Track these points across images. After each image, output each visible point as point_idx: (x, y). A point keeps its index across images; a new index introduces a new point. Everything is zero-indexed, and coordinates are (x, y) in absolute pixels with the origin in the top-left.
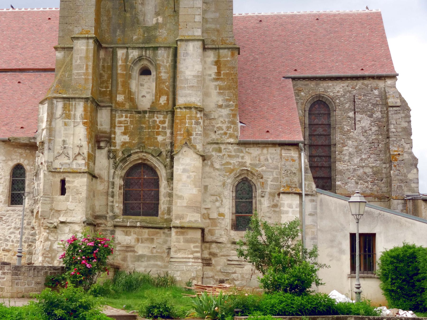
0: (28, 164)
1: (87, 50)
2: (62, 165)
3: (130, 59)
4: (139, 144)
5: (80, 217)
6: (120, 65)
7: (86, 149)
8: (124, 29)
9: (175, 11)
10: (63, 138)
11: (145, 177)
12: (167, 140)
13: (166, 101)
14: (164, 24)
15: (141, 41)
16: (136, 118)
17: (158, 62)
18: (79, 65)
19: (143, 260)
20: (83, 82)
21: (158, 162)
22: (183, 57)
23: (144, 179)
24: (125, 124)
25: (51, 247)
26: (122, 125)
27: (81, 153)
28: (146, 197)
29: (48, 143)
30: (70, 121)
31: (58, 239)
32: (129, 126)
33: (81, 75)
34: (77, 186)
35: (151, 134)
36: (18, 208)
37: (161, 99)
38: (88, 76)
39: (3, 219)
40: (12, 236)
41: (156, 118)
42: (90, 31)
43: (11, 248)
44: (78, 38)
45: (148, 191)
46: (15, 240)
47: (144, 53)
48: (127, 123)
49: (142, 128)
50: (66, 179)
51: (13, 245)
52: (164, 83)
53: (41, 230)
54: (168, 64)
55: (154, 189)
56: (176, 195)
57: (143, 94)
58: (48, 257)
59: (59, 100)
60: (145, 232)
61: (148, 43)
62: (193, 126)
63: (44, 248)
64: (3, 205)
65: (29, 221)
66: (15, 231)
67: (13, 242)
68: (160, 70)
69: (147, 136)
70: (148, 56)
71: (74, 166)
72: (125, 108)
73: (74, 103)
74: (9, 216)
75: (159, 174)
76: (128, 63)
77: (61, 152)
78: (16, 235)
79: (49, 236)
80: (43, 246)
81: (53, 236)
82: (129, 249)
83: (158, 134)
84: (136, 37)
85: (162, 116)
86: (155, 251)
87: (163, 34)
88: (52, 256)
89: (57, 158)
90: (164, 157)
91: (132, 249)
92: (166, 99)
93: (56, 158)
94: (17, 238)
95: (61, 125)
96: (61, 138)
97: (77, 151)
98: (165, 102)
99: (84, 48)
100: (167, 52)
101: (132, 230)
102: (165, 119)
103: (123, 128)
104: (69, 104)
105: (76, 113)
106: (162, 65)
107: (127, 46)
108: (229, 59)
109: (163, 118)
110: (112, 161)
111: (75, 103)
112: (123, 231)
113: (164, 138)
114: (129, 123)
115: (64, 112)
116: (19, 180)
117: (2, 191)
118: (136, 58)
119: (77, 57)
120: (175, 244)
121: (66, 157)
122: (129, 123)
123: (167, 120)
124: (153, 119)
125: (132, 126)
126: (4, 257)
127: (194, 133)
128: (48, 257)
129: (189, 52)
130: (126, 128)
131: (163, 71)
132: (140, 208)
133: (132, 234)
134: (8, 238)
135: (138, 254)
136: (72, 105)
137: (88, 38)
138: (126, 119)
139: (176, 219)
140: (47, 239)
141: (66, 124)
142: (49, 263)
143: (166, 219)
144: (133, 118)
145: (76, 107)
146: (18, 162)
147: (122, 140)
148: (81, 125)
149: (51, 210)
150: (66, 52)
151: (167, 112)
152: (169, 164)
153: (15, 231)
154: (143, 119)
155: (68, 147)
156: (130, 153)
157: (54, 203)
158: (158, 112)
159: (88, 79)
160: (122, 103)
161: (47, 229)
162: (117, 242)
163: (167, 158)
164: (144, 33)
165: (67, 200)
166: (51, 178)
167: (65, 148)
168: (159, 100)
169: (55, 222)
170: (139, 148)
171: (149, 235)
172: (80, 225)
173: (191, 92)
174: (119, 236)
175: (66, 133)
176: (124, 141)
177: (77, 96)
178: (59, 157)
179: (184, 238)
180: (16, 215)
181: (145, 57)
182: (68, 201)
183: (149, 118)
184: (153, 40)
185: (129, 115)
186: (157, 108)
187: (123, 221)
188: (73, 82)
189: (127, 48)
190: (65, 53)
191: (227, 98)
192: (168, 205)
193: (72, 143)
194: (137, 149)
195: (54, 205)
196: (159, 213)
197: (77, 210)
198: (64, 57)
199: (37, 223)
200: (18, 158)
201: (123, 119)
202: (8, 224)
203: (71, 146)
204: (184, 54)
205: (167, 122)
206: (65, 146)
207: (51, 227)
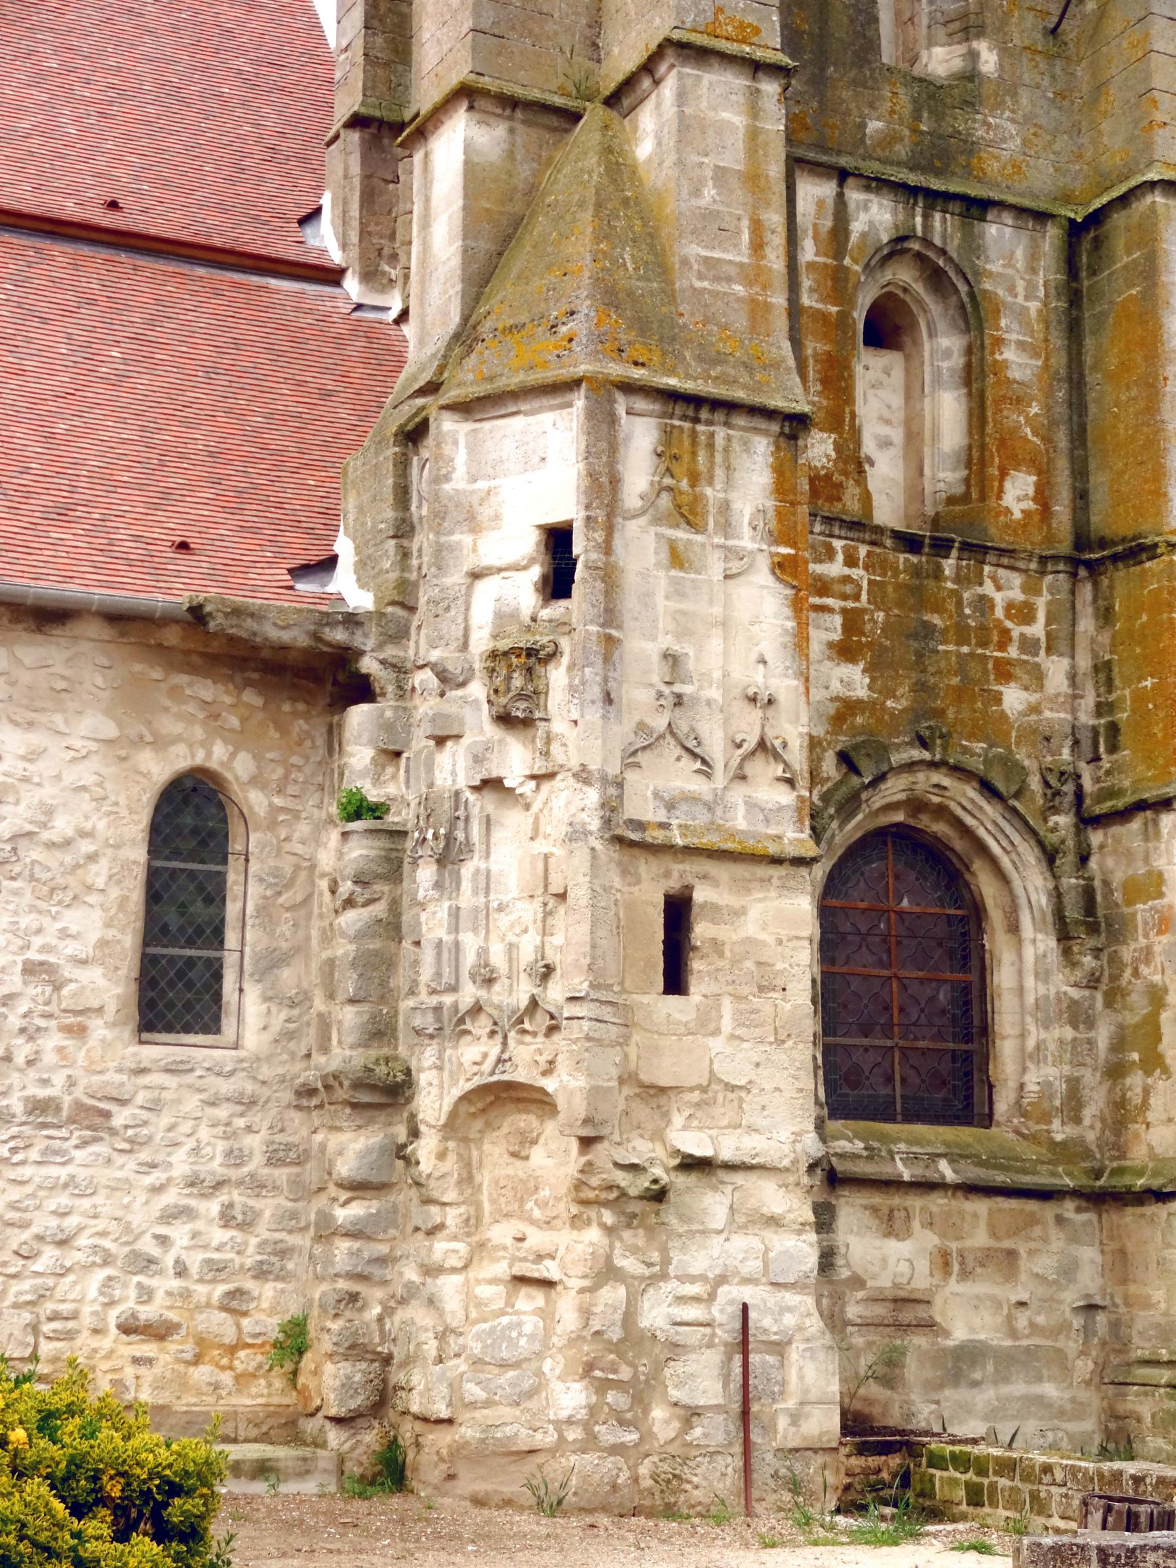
0: (256, 781)
1: (753, 134)
2: (671, 806)
3: (854, 238)
4: (917, 719)
5: (785, 1135)
6: (811, 265)
7: (796, 720)
8: (823, 70)
9: (1054, 31)
10: (666, 642)
11: (905, 903)
12: (1048, 714)
13: (1034, 499)
14: (1008, 87)
15: (901, 151)
16: (896, 572)
17: (987, 285)
18: (710, 215)
19: (977, 1376)
20: (740, 321)
23: (901, 914)
24: (844, 597)
25: (629, 1317)
26: (830, 601)
28: (914, 1019)
29: (599, 661)
30: (699, 538)
31: (672, 1270)
32: (864, 611)
33: (729, 279)
34: (763, 944)
35: (974, 669)
37: (1008, 485)
38: (764, 288)
39: (118, 1121)
40: (180, 1233)
41: (988, 588)
42: (757, 31)
43: (173, 1316)
45: (922, 981)
46: (195, 1261)
47: (919, 220)
48: (857, 597)
49: (928, 630)
51: (186, 1294)
52: (1019, 400)
53: (478, 1206)
54: (1034, 306)
55: (948, 975)
58: (619, 1385)
59: (641, 404)
60: (975, 1216)
61: (938, 173)
63: (596, 1325)
64: (108, 1034)
65: (279, 1138)
66: (193, 1203)
67: (181, 1271)
68: (998, 328)
69: (955, 681)
70: (937, 241)
71: (740, 821)
72: (844, 512)
73: (721, 433)
74: (154, 1107)
75: (987, 887)
76: (847, 261)
77: (660, 723)
78: (199, 1225)
79: (612, 1247)
80: (586, 1314)
81: (634, 1250)
83: (1005, 672)
84: (879, 125)
85: (1017, 579)
86: (1022, 1320)
87: (1004, 140)
88: (635, 1376)
89: (640, 758)
90: (1033, 800)
91: (921, 1312)
92: (1031, 491)
93: (631, 758)
94: (205, 1247)
95: (652, 559)
97: (749, 725)
98: (1030, 505)
99: (737, 119)
100: (1025, 236)
101: (915, 1202)
102: (1033, 599)
103: (838, 620)
104: (694, 434)
105: (732, 496)
106: (1004, 303)
107: (844, 161)
109: (1025, 589)
111: (729, 439)
112: (875, 1210)
113: (1034, 698)
114: (864, 596)
115: (668, 481)
116: (192, 874)
117: (103, 943)
118: (885, 238)
119: (701, 165)
121: (686, 759)
122: (864, 596)
123: (1041, 604)
125: (880, 616)
126: (130, 1371)
128: (619, 1385)
130: (852, 622)
131: (1014, 337)
132: (890, 1079)
133: (916, 1224)
134: (155, 1251)
135: (950, 1343)
136: (711, 446)
137: (756, 67)
138: (847, 571)
140: (607, 1272)
141: (677, 558)
142: (622, 1423)
143: (1064, 1144)
144: (884, 575)
145: (734, 463)
146: (199, 759)
147: (836, 688)
148: (763, 576)
150: (521, 129)
151: (1043, 560)
152: (1070, 843)
153: (193, 1203)
154: (931, 583)
155: (695, 699)
156: (885, 768)
157: (636, 1038)
158: (1002, 552)
159: (768, 307)
160: (828, 477)
161: (606, 1204)
162: (845, 1274)
164: (917, 117)
165: (706, 1024)
166: (617, 882)
167: (679, 700)
168: (1001, 490)
169: (652, 1161)
170: (924, 744)
171: (993, 1233)
172: (791, 1179)
174: (852, 1240)
175: (684, 613)
176: (844, 692)
177: (739, 395)
178: (648, 754)
180: (192, 1102)
181: (916, 246)
182: (716, 1032)
183: (957, 579)
184: (962, 160)
185: (863, 550)
186: (993, 531)
187: (872, 1155)
188: (688, 315)
189: (843, 175)
190: (512, 131)
192: (1066, 1069)
193: (717, 675)
194: (910, 744)
195: (632, 1051)
196: (1002, 1107)
197: (768, 1087)
198: (511, 155)
199: (452, 1158)
200: (198, 733)
201: (835, 568)
202: (144, 1155)
203: (715, 694)
205: (1041, 616)
206: (678, 688)
207: (633, 1192)
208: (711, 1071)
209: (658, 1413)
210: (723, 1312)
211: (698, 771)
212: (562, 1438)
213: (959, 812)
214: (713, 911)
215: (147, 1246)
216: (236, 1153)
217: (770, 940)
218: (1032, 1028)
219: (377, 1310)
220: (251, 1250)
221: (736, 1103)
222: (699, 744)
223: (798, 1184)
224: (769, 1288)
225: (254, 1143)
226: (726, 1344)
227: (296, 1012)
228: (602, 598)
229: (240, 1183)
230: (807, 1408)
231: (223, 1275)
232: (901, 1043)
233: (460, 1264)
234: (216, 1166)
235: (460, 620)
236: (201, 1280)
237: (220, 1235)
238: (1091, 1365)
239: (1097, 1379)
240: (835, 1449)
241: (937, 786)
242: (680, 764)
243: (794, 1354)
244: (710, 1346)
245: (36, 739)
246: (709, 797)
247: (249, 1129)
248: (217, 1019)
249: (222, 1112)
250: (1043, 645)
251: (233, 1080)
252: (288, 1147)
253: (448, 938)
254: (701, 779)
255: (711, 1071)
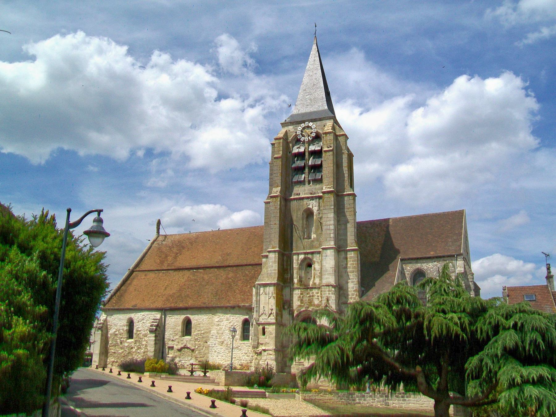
3: (299, 259)
5: (272, 347)
10: (263, 305)
25: (258, 363)
36: (246, 342)
40: (244, 357)
57: (308, 277)
82: (301, 364)
85: (317, 290)
91: (302, 364)
107: (298, 252)
108: (352, 255)
110: (291, 316)
129: (328, 254)
180: (245, 346)
202: (241, 351)
210: (266, 362)
215: (241, 358)
234: (247, 352)
237: (247, 357)
245: (233, 317)
249: (247, 347)
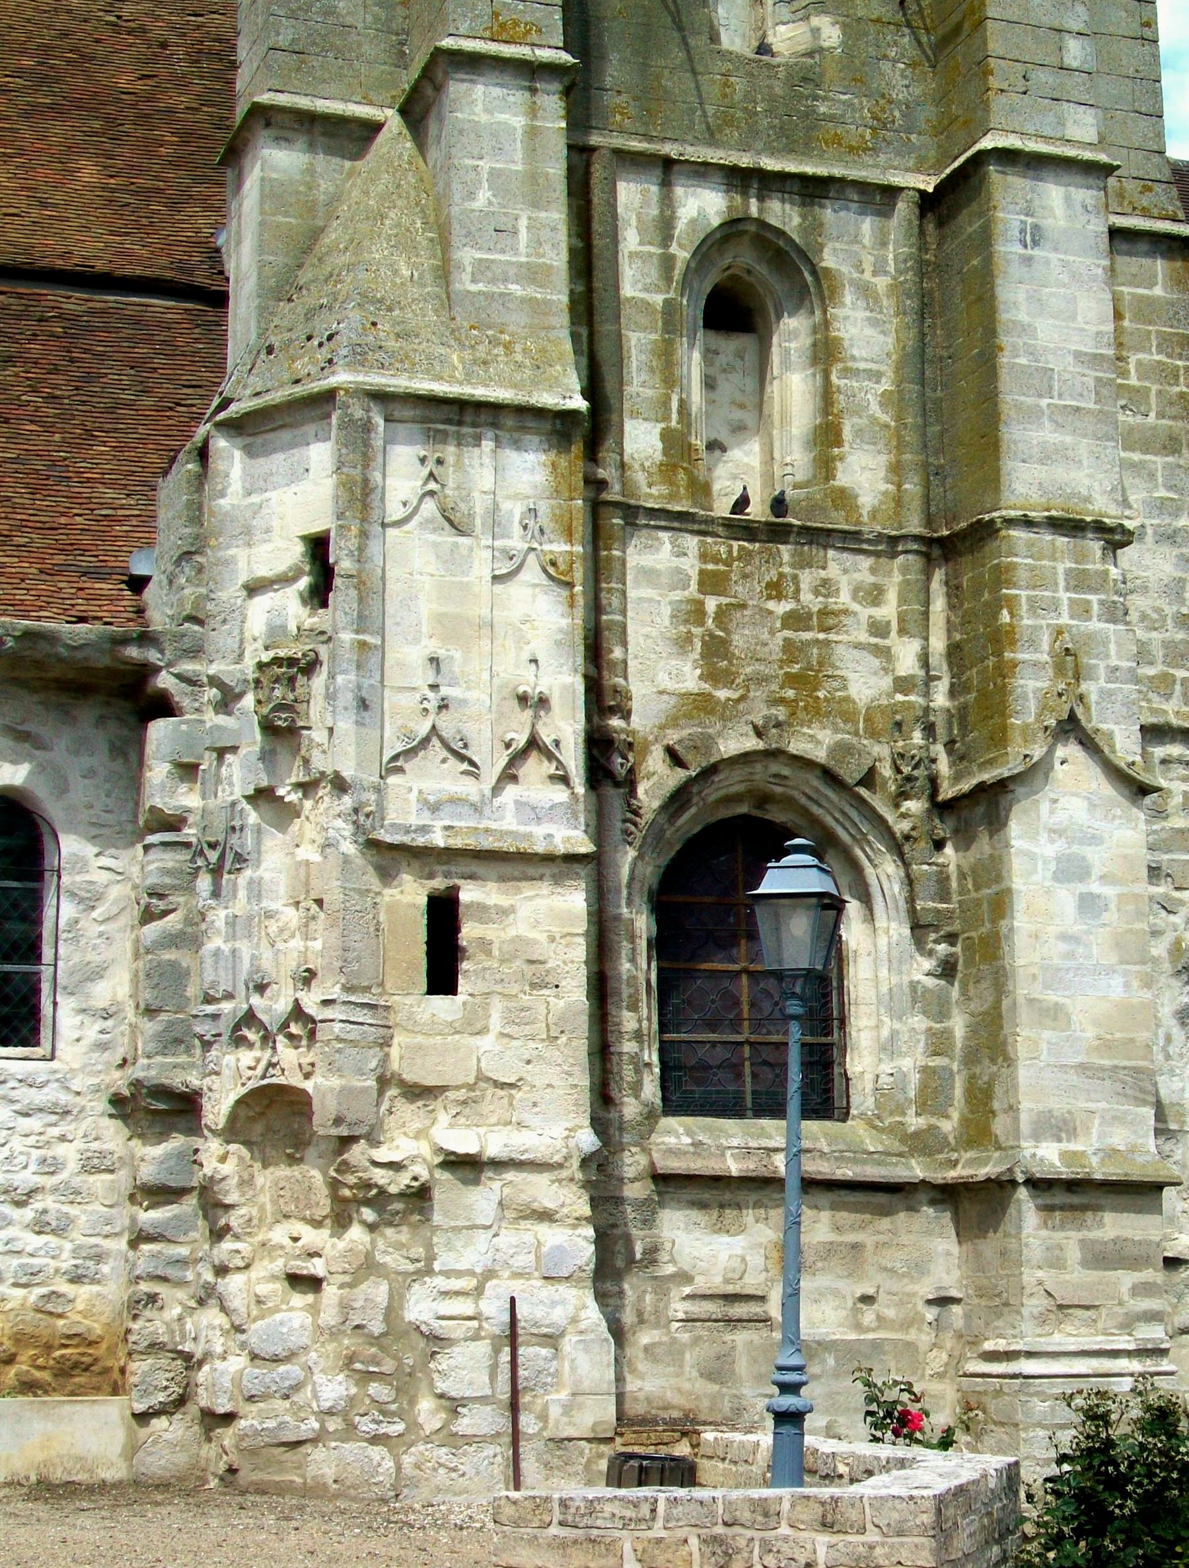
1: (532, 133)
3: (681, 226)
10: (432, 646)
21: (854, 814)
22: (1018, 249)
25: (392, 1312)
27: (548, 741)
28: (766, 1013)
31: (437, 1266)
34: (536, 942)
41: (833, 571)
44: (473, 63)
50: (465, 897)
54: (882, 283)
56: (1031, 1001)
62: (1095, 625)
76: (674, 249)
77: (423, 729)
81: (399, 1246)
82: (740, 1310)
85: (866, 562)
86: (868, 1316)
91: (753, 1309)
96: (417, 641)
107: (670, 149)
108: (1158, 291)
109: (873, 571)
115: (432, 486)
120: (1040, 1274)
121: (452, 761)
124: (823, 573)
127: (1102, 665)
129: (1047, 223)
139: (1037, 1136)
143: (917, 1134)
149: (384, 1082)
155: (463, 702)
162: (670, 1269)
163: (903, 795)
165: (474, 1025)
169: (413, 1159)
173: (1068, 439)
179: (1082, 1242)
191: (1162, 493)
197: (540, 1082)
204: (1023, 231)
205: (892, 596)
208: (479, 1069)
209: (425, 1405)
210: (494, 1309)
211: (464, 773)
212: (323, 1427)
213: (803, 800)
214: (481, 910)
216: (49, 1161)
217: (542, 938)
218: (887, 1020)
219: (177, 1311)
220: (65, 1255)
221: (506, 1100)
222: (466, 746)
223: (572, 1180)
224: (540, 1283)
225: (69, 1153)
226: (494, 1337)
227: (110, 1023)
228: (355, 606)
229: (55, 1190)
230: (580, 1399)
231: (37, 1280)
232: (753, 1038)
233: (241, 1264)
235: (236, 632)
236: (16, 1285)
237: (34, 1241)
238: (944, 1356)
239: (952, 1372)
240: (611, 1440)
241: (775, 776)
242: (445, 766)
243: (568, 1344)
244: (476, 1337)
246: (475, 798)
247: (63, 1139)
248: (36, 1031)
249: (34, 1123)
250: (894, 626)
251: (45, 1090)
252: (102, 1155)
253: (226, 948)
254: (470, 780)
255: (479, 1069)
